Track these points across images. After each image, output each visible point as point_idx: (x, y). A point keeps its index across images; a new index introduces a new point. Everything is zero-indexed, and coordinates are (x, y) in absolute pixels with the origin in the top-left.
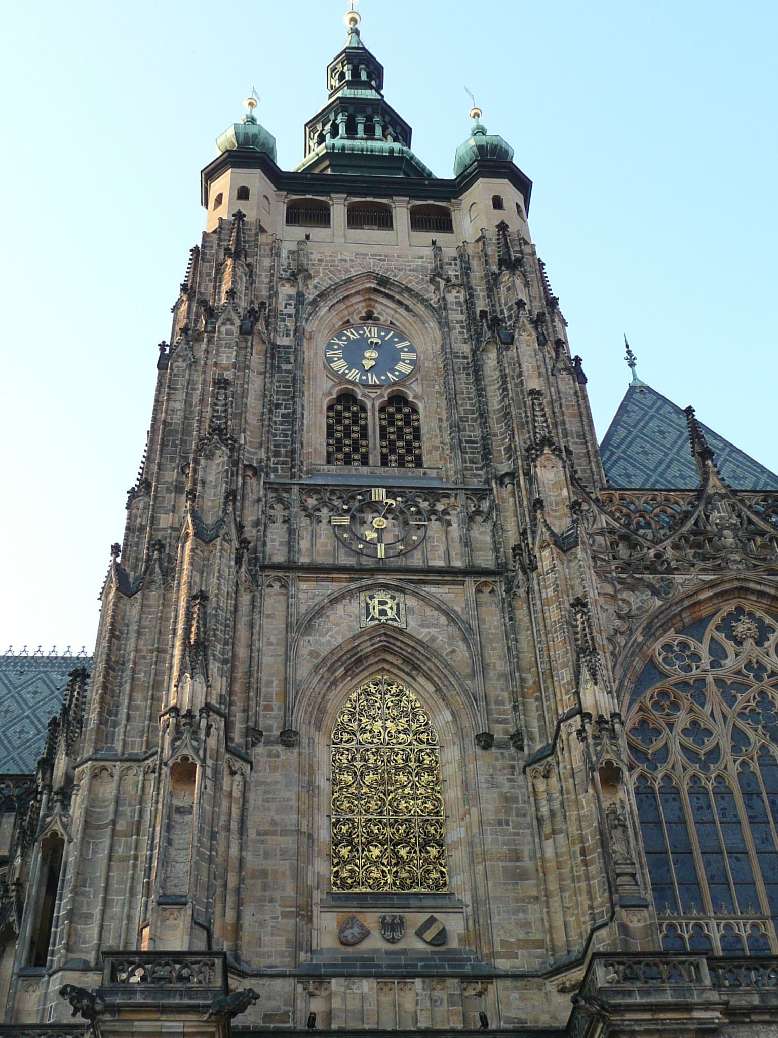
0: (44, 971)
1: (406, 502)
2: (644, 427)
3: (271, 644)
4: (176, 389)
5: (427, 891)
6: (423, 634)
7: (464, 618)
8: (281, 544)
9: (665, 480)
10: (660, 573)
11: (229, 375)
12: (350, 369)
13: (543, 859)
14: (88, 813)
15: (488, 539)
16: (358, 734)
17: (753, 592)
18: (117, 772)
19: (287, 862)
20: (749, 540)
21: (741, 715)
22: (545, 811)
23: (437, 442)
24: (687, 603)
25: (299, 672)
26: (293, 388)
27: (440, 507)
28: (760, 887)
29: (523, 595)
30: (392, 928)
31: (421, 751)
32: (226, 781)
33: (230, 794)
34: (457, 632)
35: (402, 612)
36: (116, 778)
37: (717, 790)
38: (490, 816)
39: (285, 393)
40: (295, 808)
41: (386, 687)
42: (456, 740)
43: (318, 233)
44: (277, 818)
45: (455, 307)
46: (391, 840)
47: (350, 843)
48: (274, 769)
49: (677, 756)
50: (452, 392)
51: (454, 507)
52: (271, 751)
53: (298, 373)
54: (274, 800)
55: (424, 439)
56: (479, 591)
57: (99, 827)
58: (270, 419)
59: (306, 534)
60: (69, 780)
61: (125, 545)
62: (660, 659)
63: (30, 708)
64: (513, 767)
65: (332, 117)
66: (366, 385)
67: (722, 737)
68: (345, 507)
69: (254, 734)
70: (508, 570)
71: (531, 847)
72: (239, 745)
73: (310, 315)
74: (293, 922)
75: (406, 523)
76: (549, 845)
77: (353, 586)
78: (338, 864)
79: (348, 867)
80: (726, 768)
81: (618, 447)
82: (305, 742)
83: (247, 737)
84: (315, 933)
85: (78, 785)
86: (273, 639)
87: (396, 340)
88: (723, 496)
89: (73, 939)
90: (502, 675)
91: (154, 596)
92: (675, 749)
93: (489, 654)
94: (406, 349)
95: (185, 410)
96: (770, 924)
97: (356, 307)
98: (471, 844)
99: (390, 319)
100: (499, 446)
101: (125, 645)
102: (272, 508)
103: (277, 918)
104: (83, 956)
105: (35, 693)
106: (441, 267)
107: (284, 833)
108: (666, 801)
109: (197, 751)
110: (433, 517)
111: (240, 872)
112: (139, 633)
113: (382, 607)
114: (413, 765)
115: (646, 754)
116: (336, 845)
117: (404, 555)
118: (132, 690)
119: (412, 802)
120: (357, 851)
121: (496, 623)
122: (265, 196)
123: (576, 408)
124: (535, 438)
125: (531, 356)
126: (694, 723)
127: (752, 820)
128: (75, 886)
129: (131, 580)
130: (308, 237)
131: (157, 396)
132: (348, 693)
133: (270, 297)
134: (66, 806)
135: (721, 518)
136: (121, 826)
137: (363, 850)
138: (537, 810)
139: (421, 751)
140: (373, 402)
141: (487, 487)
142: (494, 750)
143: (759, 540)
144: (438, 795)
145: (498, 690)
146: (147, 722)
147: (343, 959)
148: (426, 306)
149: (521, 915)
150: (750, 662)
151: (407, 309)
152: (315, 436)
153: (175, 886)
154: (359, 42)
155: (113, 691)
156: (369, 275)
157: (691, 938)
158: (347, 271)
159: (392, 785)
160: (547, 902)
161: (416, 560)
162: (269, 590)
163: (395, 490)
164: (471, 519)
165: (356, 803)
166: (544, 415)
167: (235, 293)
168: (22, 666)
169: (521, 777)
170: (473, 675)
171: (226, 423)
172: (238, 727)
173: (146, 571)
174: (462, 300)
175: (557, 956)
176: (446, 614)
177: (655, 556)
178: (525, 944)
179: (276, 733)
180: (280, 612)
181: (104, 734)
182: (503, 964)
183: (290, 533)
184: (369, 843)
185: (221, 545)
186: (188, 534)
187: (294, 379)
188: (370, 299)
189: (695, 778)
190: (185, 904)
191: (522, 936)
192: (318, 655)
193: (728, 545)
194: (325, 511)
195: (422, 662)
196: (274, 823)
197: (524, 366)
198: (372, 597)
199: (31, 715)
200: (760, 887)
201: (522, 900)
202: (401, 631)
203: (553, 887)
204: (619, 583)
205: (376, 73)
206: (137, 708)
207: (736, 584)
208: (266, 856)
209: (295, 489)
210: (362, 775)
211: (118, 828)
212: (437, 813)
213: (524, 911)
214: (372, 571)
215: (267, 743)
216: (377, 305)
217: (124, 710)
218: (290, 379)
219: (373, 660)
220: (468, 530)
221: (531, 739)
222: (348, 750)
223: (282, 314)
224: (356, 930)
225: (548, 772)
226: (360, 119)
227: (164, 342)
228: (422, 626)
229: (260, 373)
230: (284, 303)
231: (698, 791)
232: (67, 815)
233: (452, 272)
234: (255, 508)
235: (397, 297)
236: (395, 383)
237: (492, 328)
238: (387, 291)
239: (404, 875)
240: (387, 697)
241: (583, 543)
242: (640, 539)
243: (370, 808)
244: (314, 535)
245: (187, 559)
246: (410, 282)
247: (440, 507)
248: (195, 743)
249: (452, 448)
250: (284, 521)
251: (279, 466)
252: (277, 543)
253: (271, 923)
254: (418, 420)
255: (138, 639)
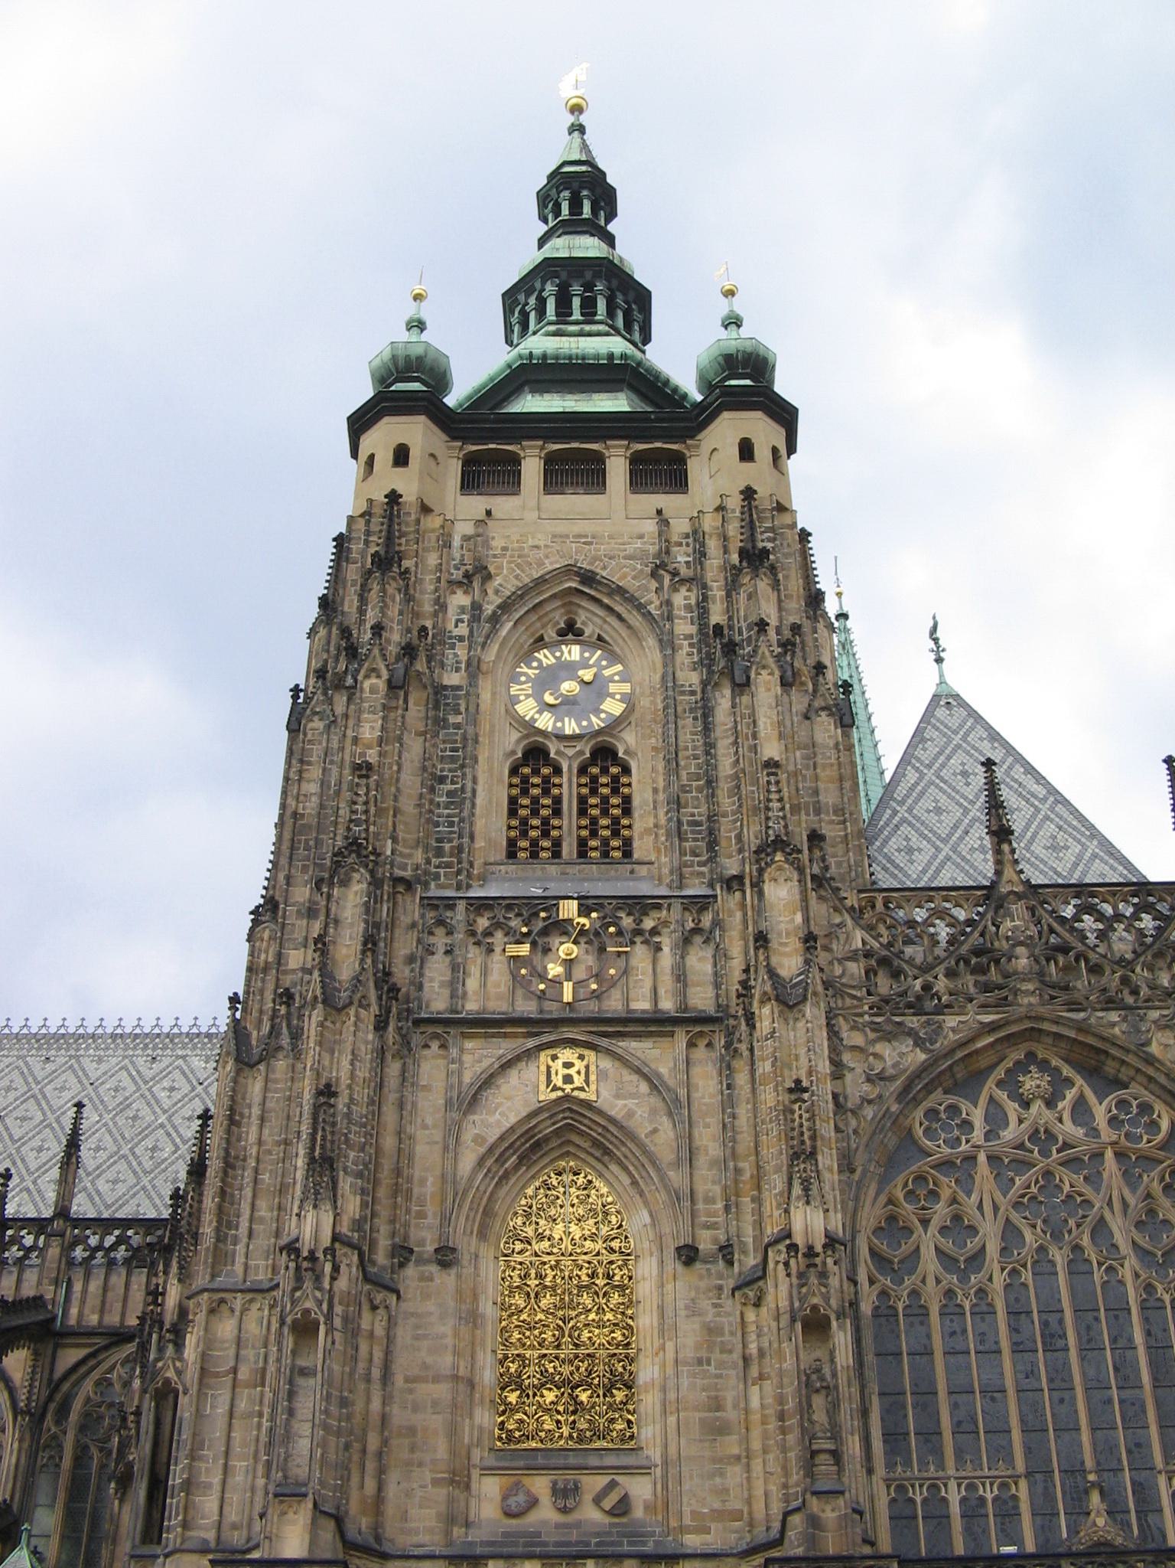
0: (159, 1551)
1: (604, 918)
2: (943, 766)
3: (425, 1127)
4: (309, 763)
5: (610, 1446)
6: (616, 1108)
7: (671, 1083)
8: (442, 985)
9: (960, 855)
10: (926, 1014)
11: (372, 755)
12: (540, 712)
13: (747, 1411)
14: (204, 1357)
15: (709, 968)
16: (534, 1242)
17: (1049, 1033)
18: (238, 1304)
19: (440, 1417)
20: (1048, 960)
21: (1017, 1205)
22: (753, 1348)
23: (651, 821)
24: (959, 1054)
25: (461, 1165)
26: (463, 755)
27: (648, 924)
28: (1016, 1435)
29: (746, 1053)
30: (566, 1495)
31: (611, 1263)
32: (366, 1321)
33: (371, 1335)
34: (660, 1105)
35: (593, 1078)
36: (237, 1313)
37: (977, 1309)
38: (688, 1353)
39: (453, 760)
40: (450, 1348)
41: (571, 1177)
42: (654, 1249)
43: (503, 505)
44: (429, 1360)
45: (683, 613)
46: (570, 1382)
47: (519, 1386)
48: (426, 1296)
49: (929, 1262)
50: (672, 749)
51: (666, 923)
52: (423, 1272)
53: (470, 730)
54: (425, 1337)
55: (636, 814)
56: (691, 1044)
57: (217, 1375)
58: (431, 802)
59: (475, 970)
60: (183, 1312)
61: (247, 992)
62: (921, 1133)
63: (165, 1112)
64: (720, 1288)
65: (538, 285)
66: (561, 737)
67: (990, 1234)
68: (524, 930)
69: (403, 1253)
70: (729, 1016)
71: (734, 1393)
72: (384, 1268)
73: (488, 637)
74: (444, 1491)
75: (602, 950)
76: (754, 1392)
77: (531, 1043)
78: (504, 1412)
79: (517, 1417)
80: (990, 1279)
81: (902, 803)
82: (465, 1259)
83: (393, 1257)
84: (473, 1502)
85: (193, 1321)
86: (429, 1121)
87: (604, 663)
88: (1019, 896)
89: (191, 1512)
90: (714, 1163)
91: (281, 1065)
92: (928, 1254)
93: (700, 1135)
94: (617, 678)
95: (321, 796)
96: (1023, 1484)
97: (551, 616)
98: (664, 1389)
99: (598, 631)
100: (727, 831)
101: (247, 1133)
102: (431, 933)
103: (425, 1487)
104: (203, 1534)
105: (172, 1089)
106: (668, 552)
107: (437, 1379)
108: (912, 1325)
109: (320, 1303)
110: (638, 940)
111: (382, 1432)
112: (262, 1119)
113: (567, 1071)
114: (600, 1282)
115: (891, 1262)
116: (503, 1389)
117: (597, 997)
118: (254, 1196)
119: (597, 1331)
120: (528, 1396)
121: (711, 1090)
122: (432, 455)
123: (836, 767)
124: (768, 835)
125: (770, 707)
126: (957, 1218)
127: (1017, 1348)
128: (192, 1450)
129: (254, 1043)
130: (489, 513)
131: (287, 771)
132: (524, 1187)
133: (435, 614)
134: (179, 1345)
135: (1015, 929)
136: (244, 1373)
137: (535, 1395)
138: (744, 1346)
139: (611, 1263)
140: (569, 759)
141: (710, 892)
142: (698, 1265)
143: (1061, 960)
144: (630, 1321)
145: (708, 1182)
146: (273, 1240)
147: (505, 1534)
148: (643, 615)
149: (718, 1480)
150: (1037, 1131)
151: (619, 617)
152: (490, 822)
153: (298, 1466)
154: (585, 147)
155: (233, 1195)
156: (569, 570)
157: (925, 1501)
158: (541, 564)
159: (574, 1309)
160: (748, 1465)
161: (614, 1004)
162: (426, 1052)
163: (590, 902)
164: (687, 941)
165: (528, 1333)
166: (780, 800)
167: (382, 628)
168: (154, 1049)
169: (730, 1302)
170: (677, 1164)
171: (367, 830)
172: (384, 1243)
173: (271, 1033)
174: (693, 602)
175: (756, 1531)
176: (646, 1077)
177: (923, 988)
178: (719, 1515)
179: (430, 1248)
180: (439, 1085)
181: (220, 1257)
182: (693, 1541)
183: (453, 970)
184: (543, 1385)
185: (357, 1016)
186: (316, 997)
187: (465, 738)
188: (571, 603)
189: (949, 1293)
190: (305, 1495)
191: (717, 1505)
192: (484, 1140)
193: (1020, 969)
194: (499, 935)
195: (615, 1146)
196: (425, 1366)
197: (761, 723)
198: (554, 1058)
199: (166, 1122)
200: (1016, 1435)
201: (720, 1460)
202: (587, 1104)
203: (756, 1445)
204: (873, 1030)
205: (605, 199)
206: (262, 1220)
207: (1028, 1025)
208: (416, 1408)
209: (461, 906)
210: (537, 1295)
211: (240, 1376)
212: (628, 1344)
213: (722, 1475)
214: (556, 1023)
215: (421, 1261)
216: (581, 611)
217: (244, 1224)
218: (458, 738)
219: (554, 1143)
220: (682, 957)
221: (745, 1252)
222: (521, 1263)
223: (450, 638)
224: (521, 1498)
225: (759, 1298)
226: (576, 288)
227: (297, 686)
228: (617, 1096)
229: (419, 734)
230: (454, 619)
231: (951, 1310)
232: (181, 1359)
233: (681, 557)
234: (409, 936)
235: (606, 601)
236: (600, 732)
237: (725, 655)
238: (593, 593)
239: (582, 1425)
240: (573, 1190)
241: (815, 994)
242: (905, 966)
243: (544, 1340)
244: (485, 972)
245: (313, 1033)
246: (624, 576)
247: (648, 924)
248: (318, 1294)
249: (668, 835)
250: (447, 952)
251: (442, 871)
252: (436, 985)
253: (419, 1493)
254: (629, 785)
255: (261, 1127)
